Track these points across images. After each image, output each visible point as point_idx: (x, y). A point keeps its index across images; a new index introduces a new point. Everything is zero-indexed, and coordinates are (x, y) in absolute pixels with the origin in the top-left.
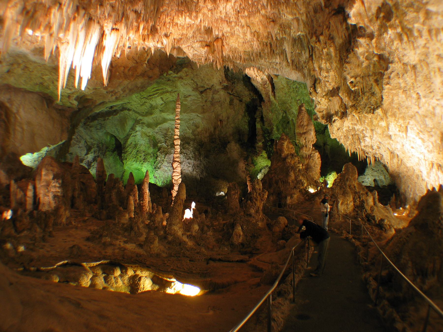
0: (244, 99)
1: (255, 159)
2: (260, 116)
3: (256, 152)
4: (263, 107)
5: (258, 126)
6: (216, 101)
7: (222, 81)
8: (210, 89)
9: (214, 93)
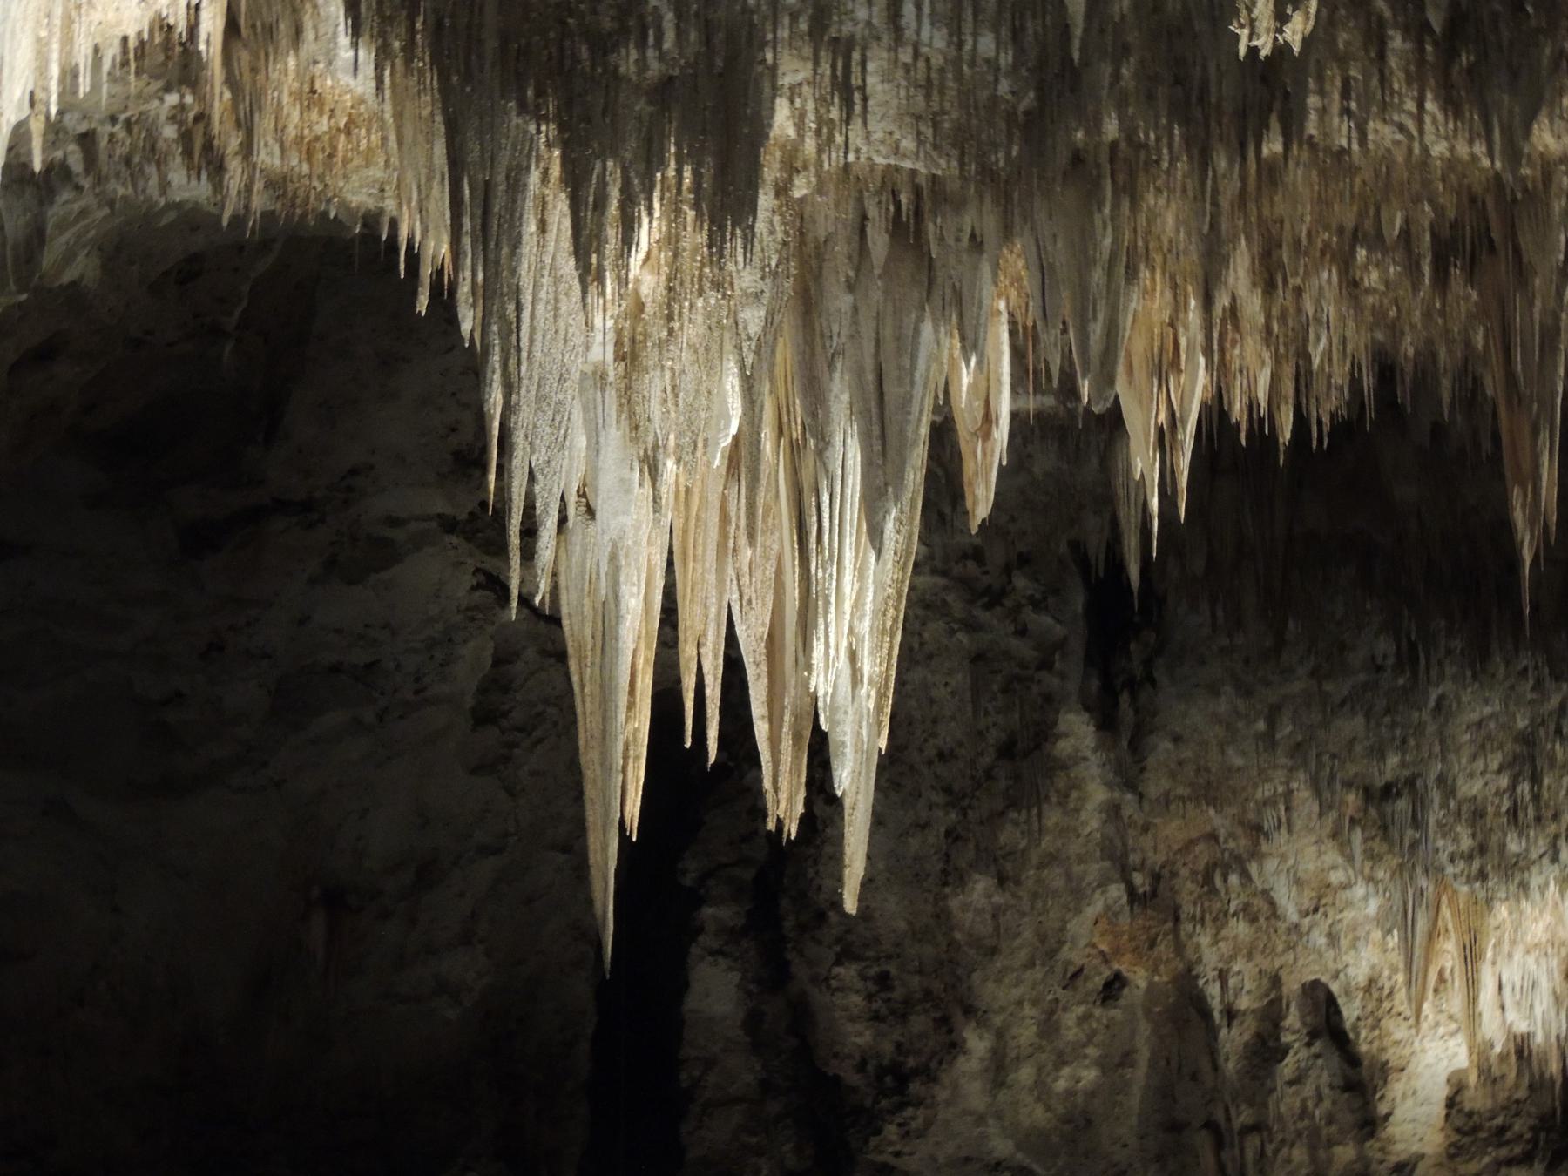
2: (748, 874)
5: (715, 991)
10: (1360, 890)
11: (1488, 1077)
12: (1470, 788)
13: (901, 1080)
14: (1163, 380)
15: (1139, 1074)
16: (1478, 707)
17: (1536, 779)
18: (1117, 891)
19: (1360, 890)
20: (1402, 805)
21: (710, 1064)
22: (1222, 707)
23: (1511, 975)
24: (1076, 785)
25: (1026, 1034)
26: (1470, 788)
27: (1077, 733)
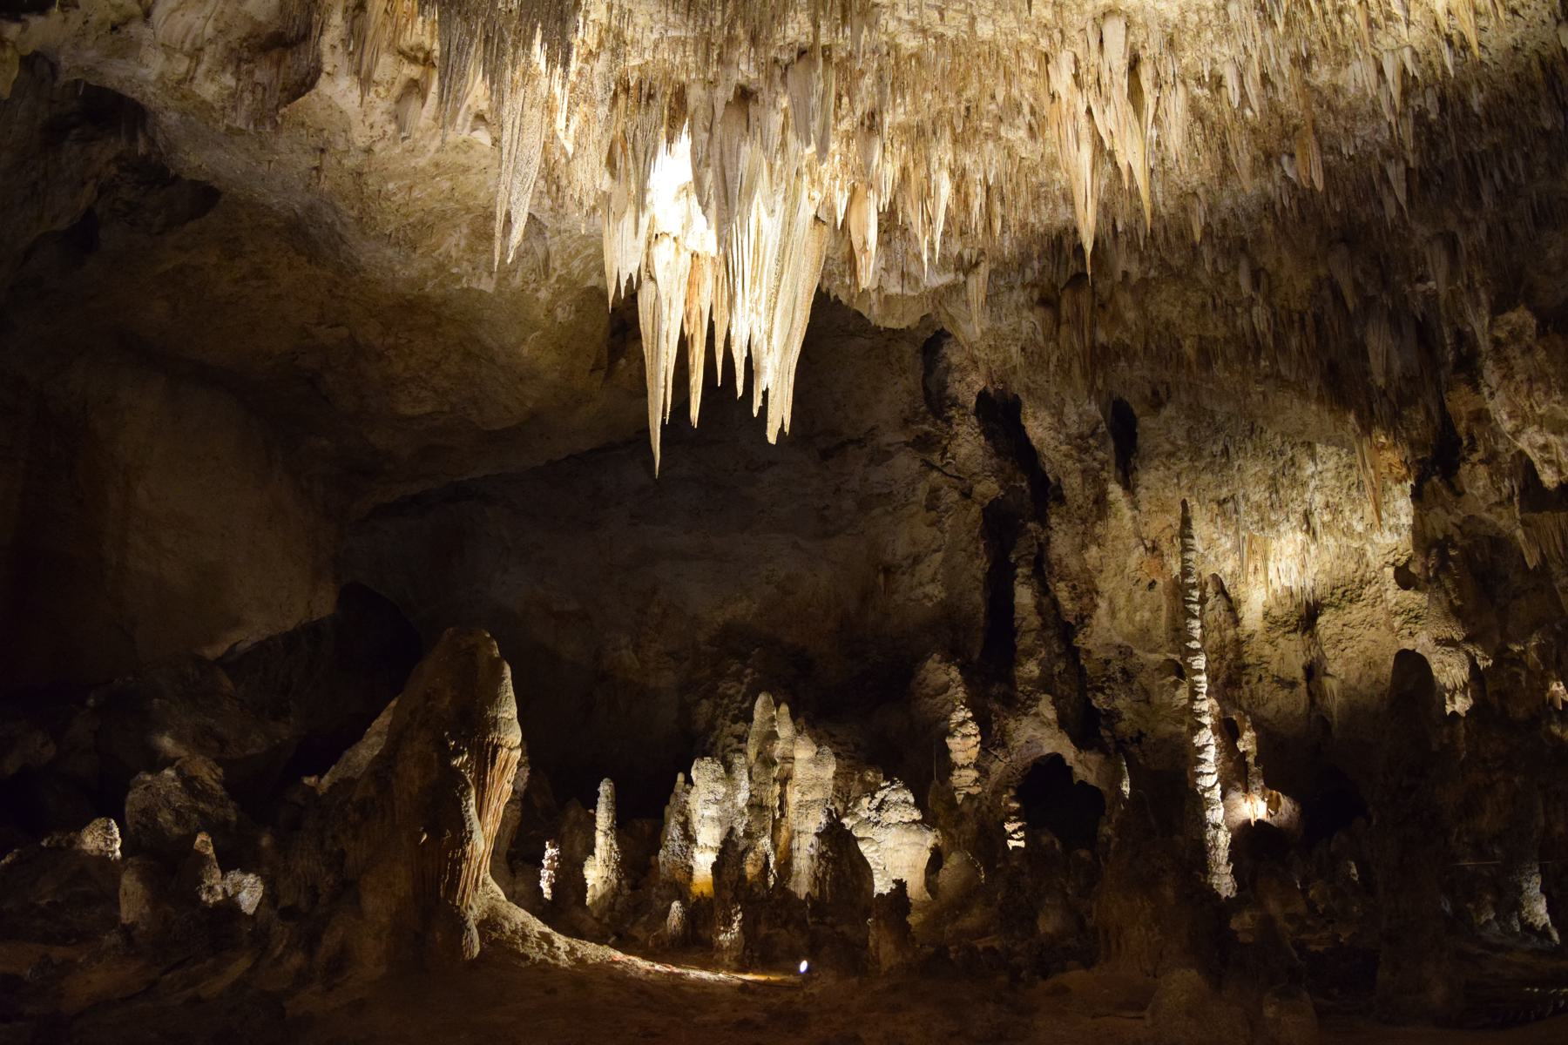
0: (980, 488)
1: (1012, 724)
3: (1018, 701)
4: (1054, 520)
5: (1024, 596)
6: (876, 491)
7: (916, 414)
8: (860, 441)
9: (871, 460)
10: (1223, 540)
11: (1280, 604)
12: (1255, 498)
13: (1084, 618)
14: (924, 201)
15: (1164, 613)
16: (1253, 468)
17: (1277, 492)
18: (1142, 548)
19: (1223, 540)
20: (1230, 505)
21: (1024, 619)
22: (1161, 474)
23: (1282, 566)
24: (1119, 510)
25: (1121, 601)
26: (1255, 498)
27: (1115, 491)
